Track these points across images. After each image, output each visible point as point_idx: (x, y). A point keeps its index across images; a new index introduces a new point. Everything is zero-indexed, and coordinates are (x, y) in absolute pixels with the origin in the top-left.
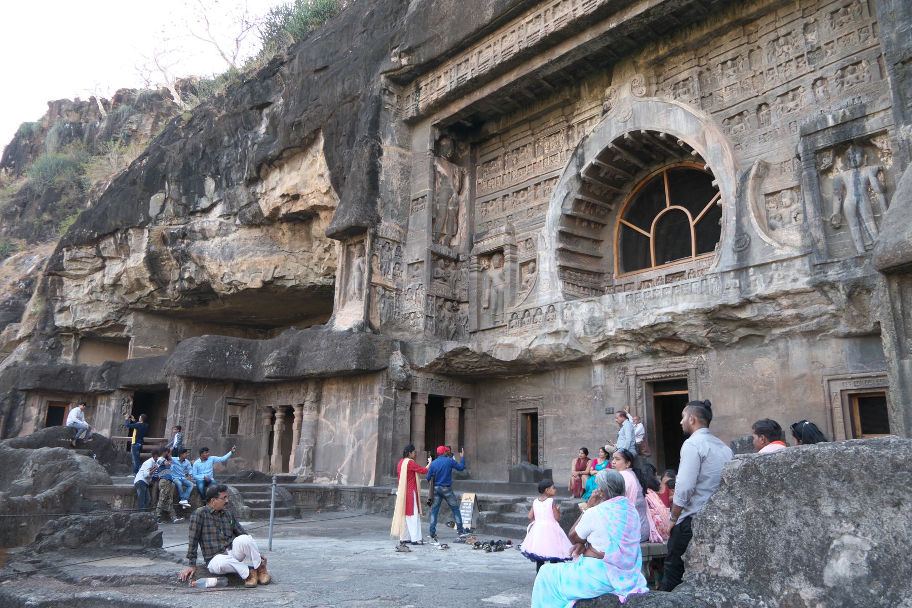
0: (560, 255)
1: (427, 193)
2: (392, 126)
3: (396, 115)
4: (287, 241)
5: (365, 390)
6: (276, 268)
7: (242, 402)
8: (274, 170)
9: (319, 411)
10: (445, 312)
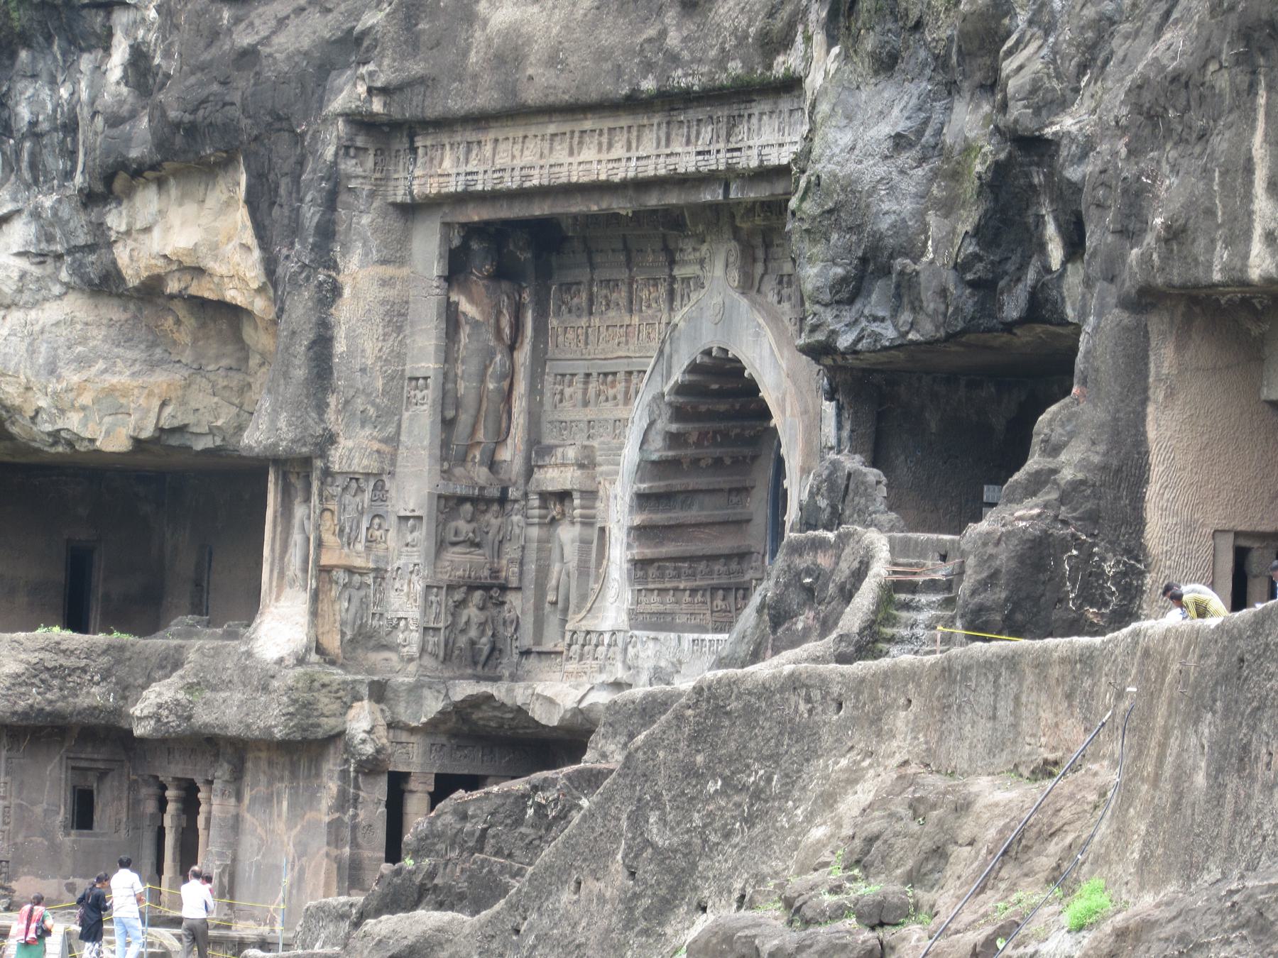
0: (638, 538)
1: (431, 373)
2: (363, 221)
3: (372, 195)
4: (188, 340)
5: (310, 769)
6: (164, 404)
7: (101, 765)
8: (145, 186)
9: (239, 797)
10: (472, 612)
